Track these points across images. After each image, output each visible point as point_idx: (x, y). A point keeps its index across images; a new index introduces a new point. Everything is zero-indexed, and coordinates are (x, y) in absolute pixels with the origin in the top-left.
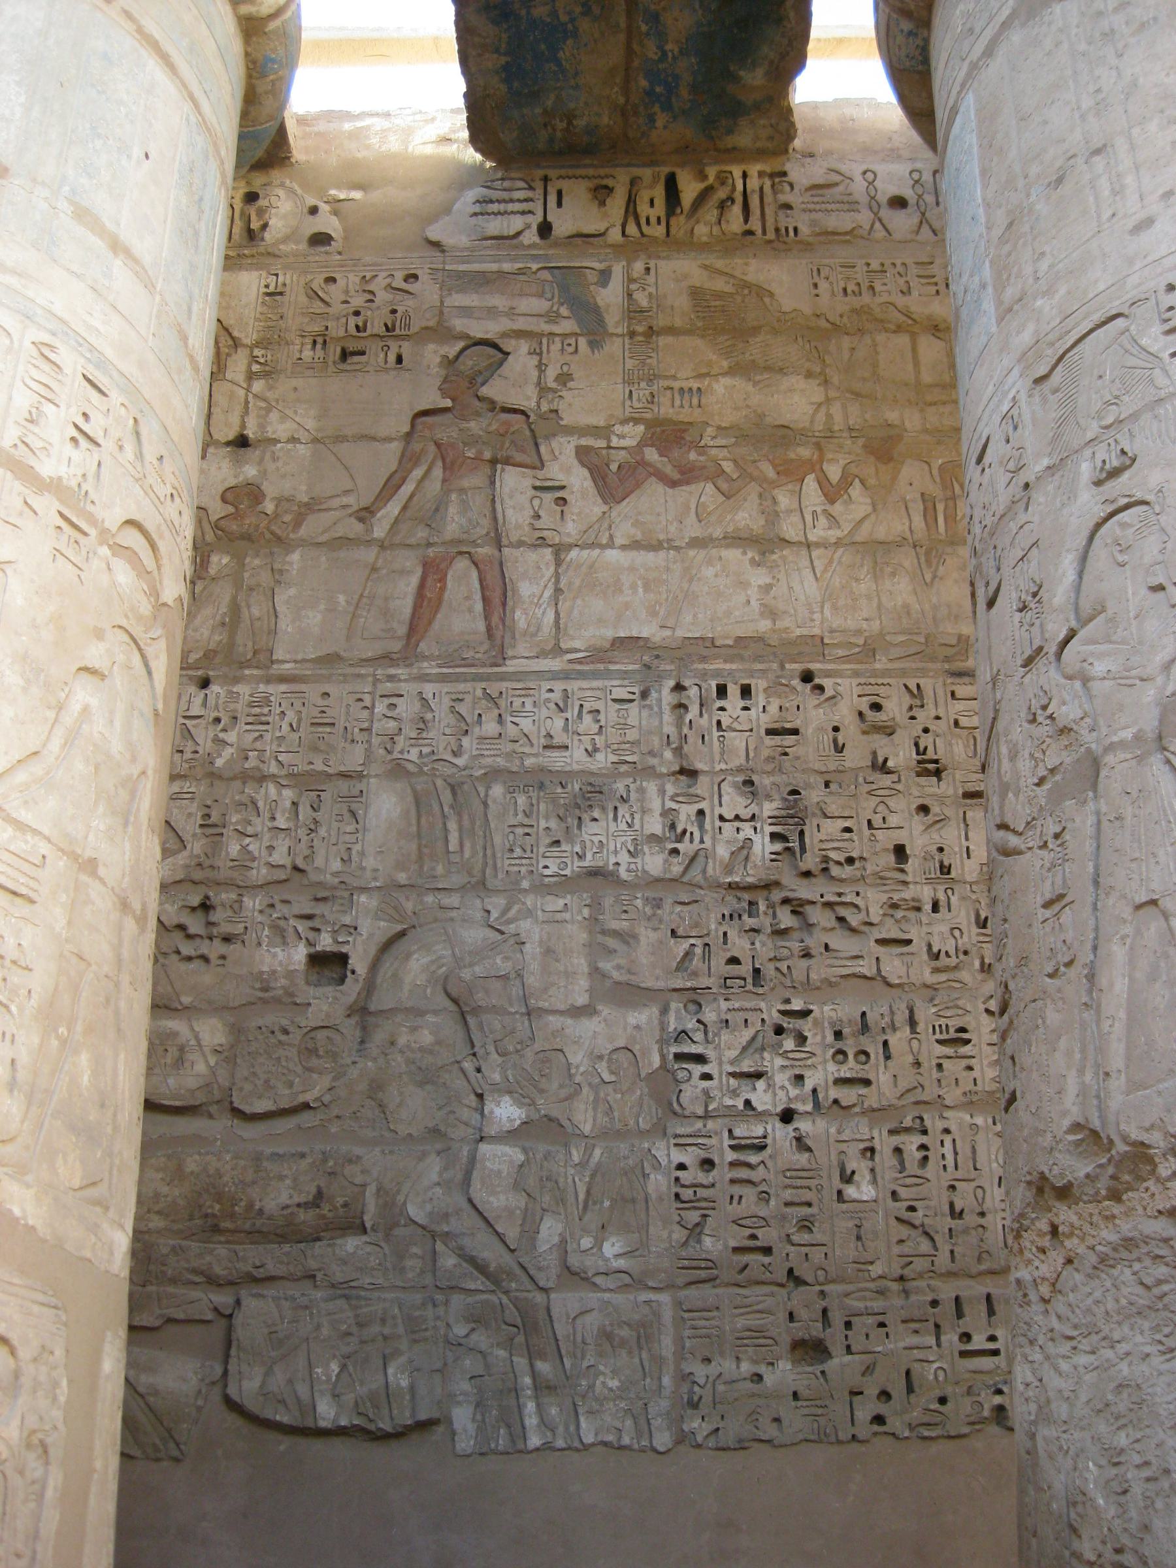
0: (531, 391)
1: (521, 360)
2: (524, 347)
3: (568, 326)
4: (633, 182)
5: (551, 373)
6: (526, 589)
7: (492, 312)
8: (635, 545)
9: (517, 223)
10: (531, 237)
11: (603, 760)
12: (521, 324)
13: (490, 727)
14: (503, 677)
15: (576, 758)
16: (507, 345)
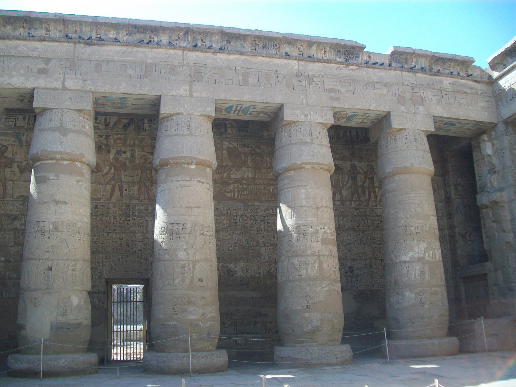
0: (11, 155)
1: (10, 149)
2: (11, 147)
3: (17, 143)
4: (29, 116)
5: (14, 152)
6: (9, 187)
7: (6, 140)
8: (24, 181)
9: (11, 123)
10: (13, 126)
11: (17, 213)
12: (10, 143)
13: (3, 208)
14: (5, 201)
15: (14, 213)
16: (8, 146)
